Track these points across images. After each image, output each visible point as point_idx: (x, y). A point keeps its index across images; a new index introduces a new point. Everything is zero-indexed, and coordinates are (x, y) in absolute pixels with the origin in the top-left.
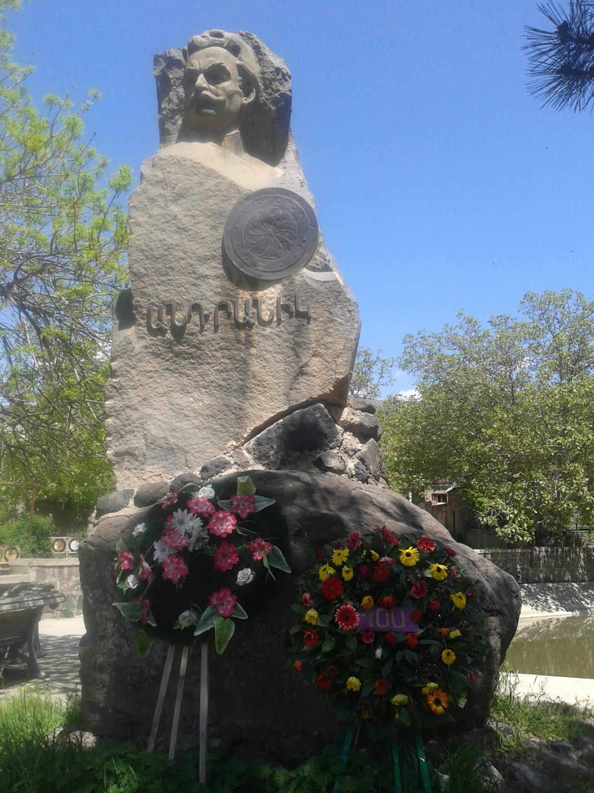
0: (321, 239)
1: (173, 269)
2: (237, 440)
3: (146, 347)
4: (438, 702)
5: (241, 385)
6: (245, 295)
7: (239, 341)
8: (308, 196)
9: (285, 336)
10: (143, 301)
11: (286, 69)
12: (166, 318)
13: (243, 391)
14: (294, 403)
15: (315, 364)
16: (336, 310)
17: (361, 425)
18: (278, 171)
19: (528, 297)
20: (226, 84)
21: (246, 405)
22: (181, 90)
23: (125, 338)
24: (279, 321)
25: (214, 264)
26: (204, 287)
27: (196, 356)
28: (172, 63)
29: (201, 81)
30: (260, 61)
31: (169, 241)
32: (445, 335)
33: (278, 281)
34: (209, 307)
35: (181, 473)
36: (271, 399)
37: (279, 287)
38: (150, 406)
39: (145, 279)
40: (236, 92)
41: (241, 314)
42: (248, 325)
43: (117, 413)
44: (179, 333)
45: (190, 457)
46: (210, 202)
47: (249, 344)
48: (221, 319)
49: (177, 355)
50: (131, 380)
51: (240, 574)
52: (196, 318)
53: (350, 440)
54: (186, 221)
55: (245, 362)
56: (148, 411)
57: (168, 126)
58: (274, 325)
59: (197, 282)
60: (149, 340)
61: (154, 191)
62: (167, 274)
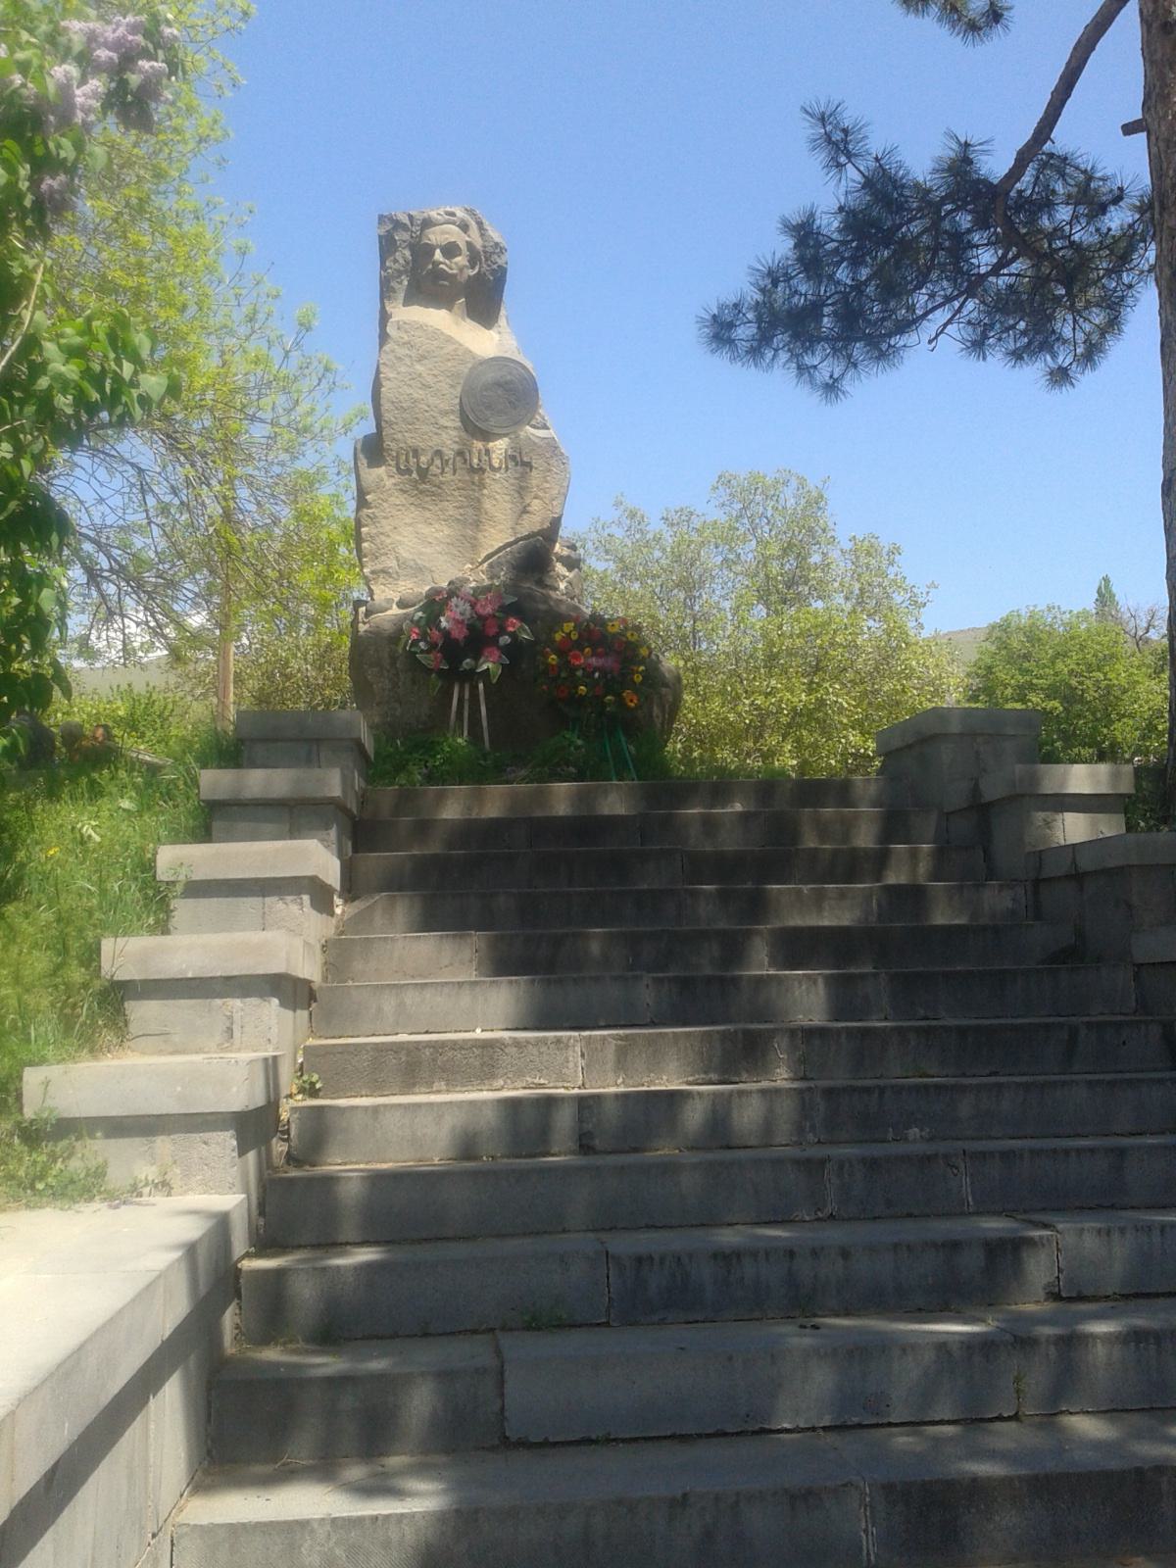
0: (540, 403)
1: (418, 419)
2: (472, 564)
3: (395, 485)
4: (631, 701)
5: (474, 519)
6: (479, 445)
7: (473, 483)
8: (529, 365)
9: (513, 481)
10: (393, 445)
11: (504, 244)
12: (413, 461)
13: (477, 524)
14: (519, 536)
15: (536, 505)
16: (553, 462)
17: (569, 557)
18: (493, 333)
19: (724, 480)
20: (458, 259)
21: (480, 535)
22: (407, 253)
23: (378, 476)
24: (507, 468)
25: (452, 417)
26: (444, 435)
27: (437, 494)
28: (398, 225)
29: (438, 255)
30: (482, 235)
31: (416, 395)
32: (594, 536)
33: (505, 435)
34: (449, 454)
35: (427, 588)
36: (501, 531)
37: (506, 439)
38: (400, 534)
39: (395, 427)
40: (466, 266)
41: (476, 461)
42: (482, 470)
43: (372, 539)
44: (423, 473)
45: (436, 576)
46: (449, 364)
47: (482, 485)
48: (459, 464)
49: (421, 492)
50: (383, 511)
51: (501, 639)
52: (438, 462)
53: (560, 568)
54: (430, 380)
55: (479, 501)
56: (398, 538)
57: (393, 284)
58: (502, 471)
59: (439, 431)
60: (397, 478)
61: (402, 351)
62: (414, 423)
